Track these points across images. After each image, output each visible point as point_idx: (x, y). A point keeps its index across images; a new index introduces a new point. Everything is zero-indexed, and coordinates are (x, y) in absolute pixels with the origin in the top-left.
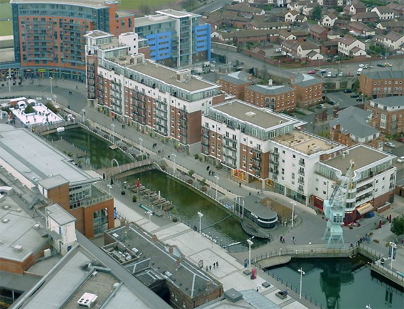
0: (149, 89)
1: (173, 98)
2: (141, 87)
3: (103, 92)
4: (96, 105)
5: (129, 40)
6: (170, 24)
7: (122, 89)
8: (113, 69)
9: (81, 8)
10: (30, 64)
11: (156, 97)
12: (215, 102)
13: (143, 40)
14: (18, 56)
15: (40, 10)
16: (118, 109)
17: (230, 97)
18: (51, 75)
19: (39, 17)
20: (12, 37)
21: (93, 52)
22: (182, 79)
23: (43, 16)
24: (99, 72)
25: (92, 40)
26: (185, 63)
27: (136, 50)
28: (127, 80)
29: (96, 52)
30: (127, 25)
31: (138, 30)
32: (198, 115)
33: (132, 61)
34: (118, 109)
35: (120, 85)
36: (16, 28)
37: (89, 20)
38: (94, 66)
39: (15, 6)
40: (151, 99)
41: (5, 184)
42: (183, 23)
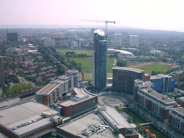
0: (153, 100)
1: (161, 104)
2: (151, 99)
3: (138, 99)
5: (148, 83)
7: (145, 99)
12: (174, 107)
17: (179, 106)
20: (112, 78)
24: (138, 93)
26: (165, 92)
30: (148, 78)
31: (152, 81)
32: (169, 110)
33: (149, 90)
34: (143, 105)
35: (144, 98)
38: (137, 91)
40: (153, 104)
41: (107, 125)
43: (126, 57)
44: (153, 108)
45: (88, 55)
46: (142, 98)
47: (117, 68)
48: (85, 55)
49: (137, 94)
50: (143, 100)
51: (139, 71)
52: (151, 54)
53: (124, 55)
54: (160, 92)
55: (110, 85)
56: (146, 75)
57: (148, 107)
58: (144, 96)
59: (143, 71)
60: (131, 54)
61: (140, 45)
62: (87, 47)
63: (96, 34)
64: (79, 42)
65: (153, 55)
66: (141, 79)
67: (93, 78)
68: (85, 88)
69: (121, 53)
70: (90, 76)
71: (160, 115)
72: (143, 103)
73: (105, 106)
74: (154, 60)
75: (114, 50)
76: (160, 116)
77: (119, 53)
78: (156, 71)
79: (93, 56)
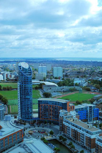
1: (87, 133)
2: (76, 129)
3: (64, 129)
4: (62, 133)
5: (73, 113)
6: (86, 108)
7: (70, 129)
8: (68, 122)
9: (59, 102)
10: (43, 119)
11: (81, 132)
13: (77, 113)
14: (39, 116)
15: (46, 102)
16: (69, 135)
18: (49, 122)
19: (46, 105)
20: (37, 110)
21: (62, 117)
22: (89, 127)
23: (47, 105)
25: (62, 112)
27: (75, 117)
28: (72, 126)
29: (62, 117)
30: (72, 108)
36: (39, 106)
37: (61, 106)
38: (62, 121)
39: (39, 101)
40: (79, 133)
42: (90, 108)
43: (51, 89)
44: (79, 138)
45: (13, 88)
46: (68, 128)
47: (42, 99)
48: (11, 87)
49: (63, 125)
50: (68, 130)
51: (64, 101)
52: (74, 84)
53: (49, 86)
54: (86, 120)
55: (36, 116)
56: (71, 105)
57: (74, 137)
58: (70, 126)
59: (67, 101)
60: (56, 85)
61: (64, 76)
62: (12, 80)
63: (20, 66)
64: (4, 75)
65: (76, 85)
66: (66, 109)
67: (19, 110)
68: (11, 121)
69: (45, 85)
70: (17, 108)
71: (87, 144)
72: (69, 133)
73: (31, 139)
74: (78, 90)
75: (39, 81)
76: (87, 146)
77: (44, 84)
78: (80, 100)
79: (18, 89)
